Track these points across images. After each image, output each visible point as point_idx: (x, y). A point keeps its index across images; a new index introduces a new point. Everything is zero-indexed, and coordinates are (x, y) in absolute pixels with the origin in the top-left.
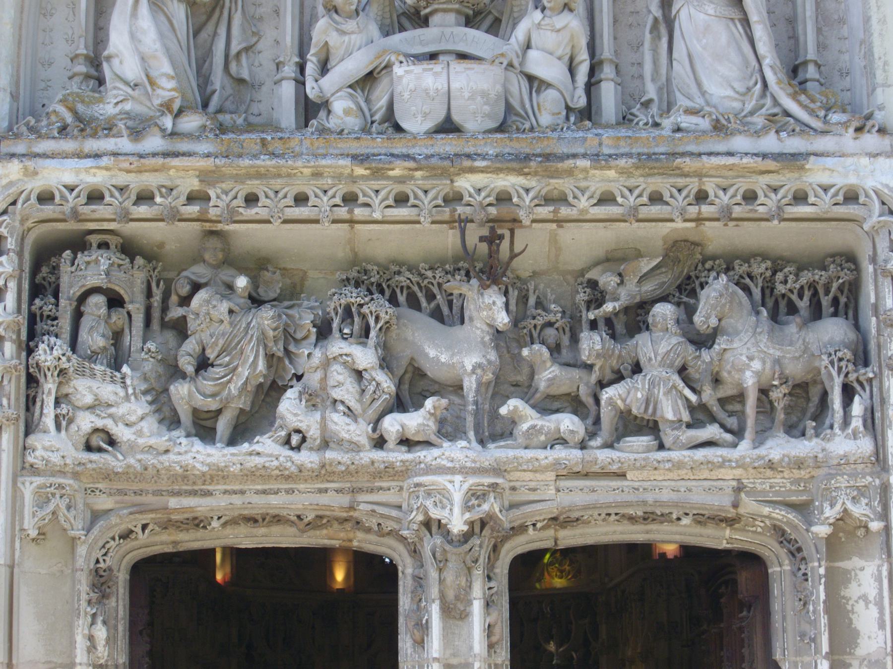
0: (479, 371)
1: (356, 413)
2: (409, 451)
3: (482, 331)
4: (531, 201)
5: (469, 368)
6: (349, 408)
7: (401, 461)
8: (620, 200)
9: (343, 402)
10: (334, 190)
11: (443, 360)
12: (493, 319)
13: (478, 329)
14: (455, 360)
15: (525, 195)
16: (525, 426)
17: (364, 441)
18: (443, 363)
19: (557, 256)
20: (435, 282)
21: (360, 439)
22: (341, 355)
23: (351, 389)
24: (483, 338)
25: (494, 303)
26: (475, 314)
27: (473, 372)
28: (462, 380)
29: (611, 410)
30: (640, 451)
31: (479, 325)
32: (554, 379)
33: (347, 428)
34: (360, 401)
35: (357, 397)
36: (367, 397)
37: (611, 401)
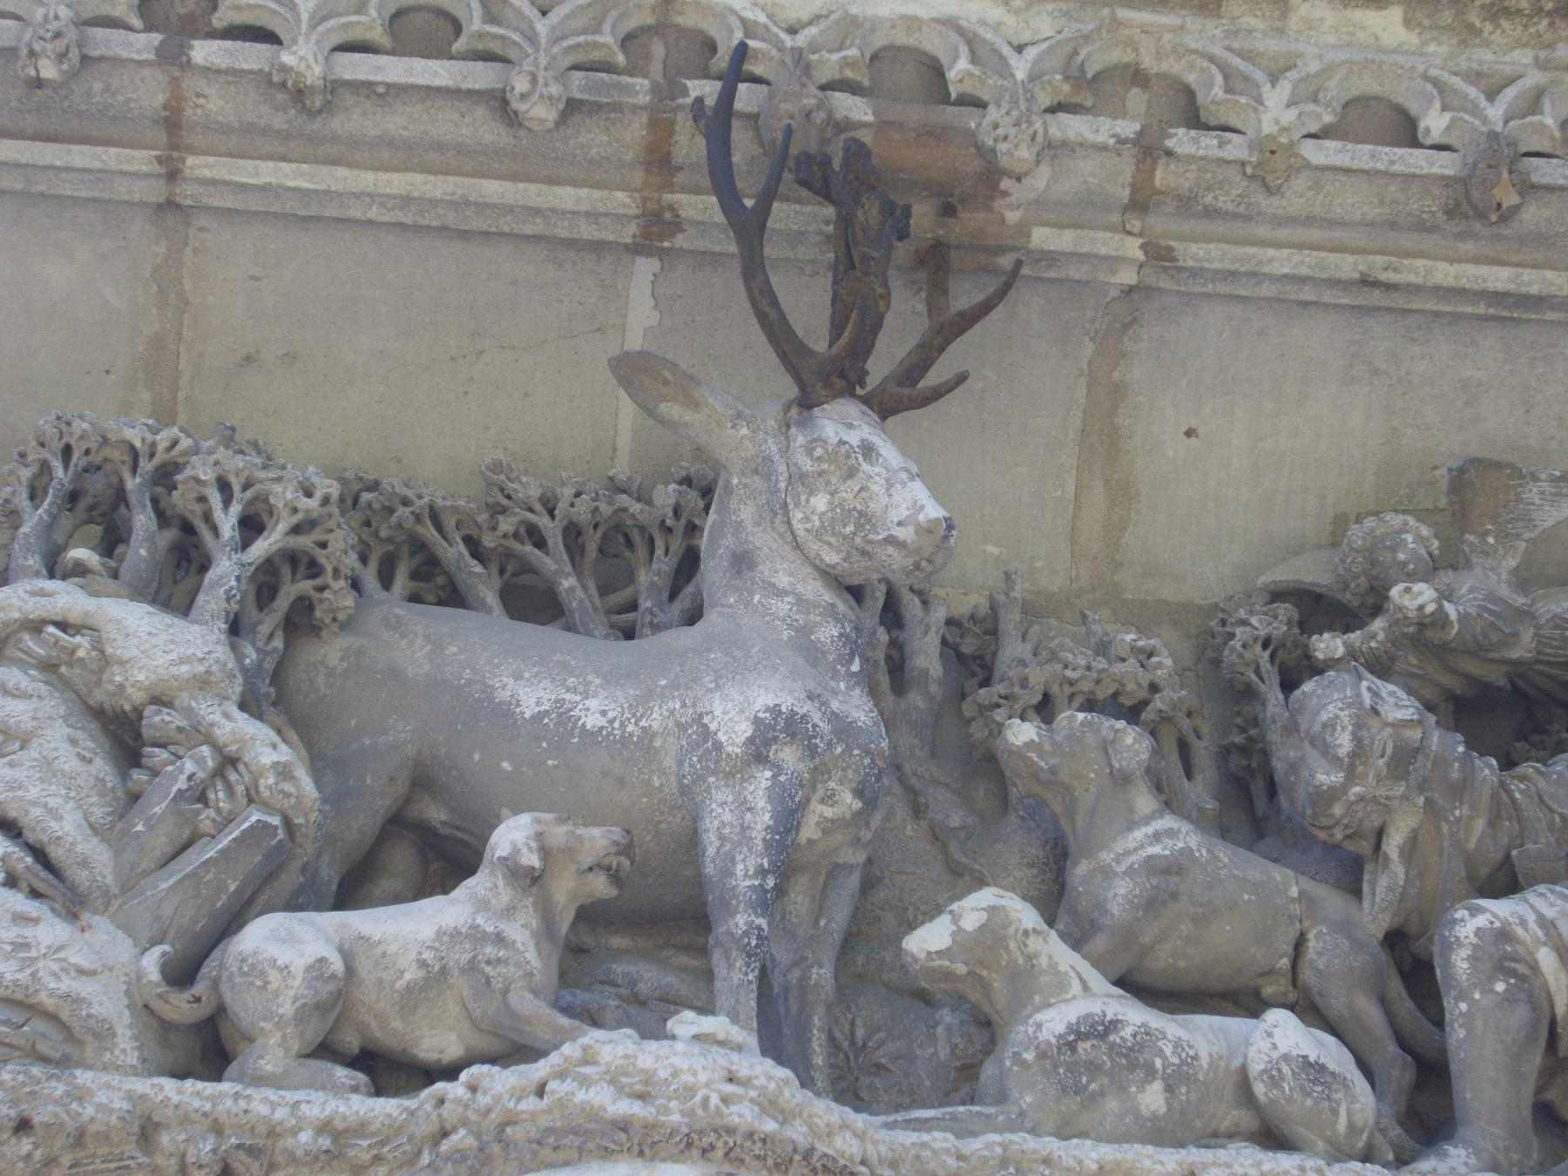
0: (789, 756)
1: (81, 877)
2: (379, 1091)
5: (734, 731)
6: (39, 854)
7: (324, 1127)
8: (1434, 123)
11: (592, 721)
12: (866, 519)
16: (1054, 1021)
17: (107, 1002)
18: (590, 736)
21: (84, 987)
22: (36, 627)
23: (68, 760)
24: (804, 631)
26: (763, 540)
27: (758, 752)
29: (1509, 999)
31: (783, 581)
34: (111, 831)
35: (99, 813)
36: (157, 816)
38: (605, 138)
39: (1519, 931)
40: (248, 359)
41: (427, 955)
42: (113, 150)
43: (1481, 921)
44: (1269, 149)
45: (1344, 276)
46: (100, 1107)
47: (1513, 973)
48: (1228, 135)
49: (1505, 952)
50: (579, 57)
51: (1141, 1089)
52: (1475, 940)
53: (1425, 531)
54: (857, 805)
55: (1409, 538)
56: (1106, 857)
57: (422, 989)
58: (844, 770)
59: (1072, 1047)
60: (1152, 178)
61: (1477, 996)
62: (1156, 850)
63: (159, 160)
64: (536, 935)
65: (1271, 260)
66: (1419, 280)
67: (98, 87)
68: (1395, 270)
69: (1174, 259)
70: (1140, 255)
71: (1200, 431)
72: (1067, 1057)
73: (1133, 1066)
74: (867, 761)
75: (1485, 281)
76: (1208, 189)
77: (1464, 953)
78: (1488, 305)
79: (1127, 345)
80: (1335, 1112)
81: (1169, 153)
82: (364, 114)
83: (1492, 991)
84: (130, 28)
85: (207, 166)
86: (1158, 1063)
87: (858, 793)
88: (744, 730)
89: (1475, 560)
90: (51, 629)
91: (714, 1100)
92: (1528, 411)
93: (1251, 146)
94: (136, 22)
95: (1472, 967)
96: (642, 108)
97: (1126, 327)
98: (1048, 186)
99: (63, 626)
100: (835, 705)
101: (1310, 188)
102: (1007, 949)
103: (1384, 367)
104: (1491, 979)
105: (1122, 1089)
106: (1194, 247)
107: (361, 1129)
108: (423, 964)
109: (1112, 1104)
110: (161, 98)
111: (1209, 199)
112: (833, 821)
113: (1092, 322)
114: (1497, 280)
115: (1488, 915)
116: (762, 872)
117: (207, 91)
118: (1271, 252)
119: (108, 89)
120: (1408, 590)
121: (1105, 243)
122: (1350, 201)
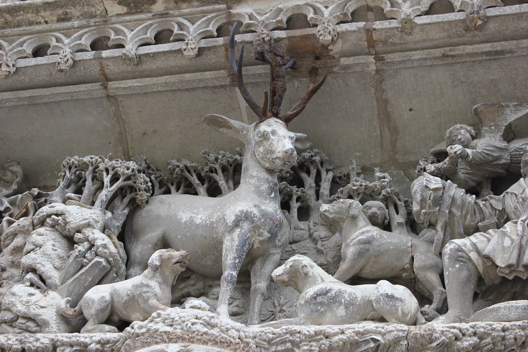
1: (48, 281)
3: (259, 179)
4: (331, 15)
5: (230, 219)
7: (99, 342)
9: (34, 271)
10: (80, 32)
11: (198, 221)
13: (253, 177)
14: (214, 219)
15: (323, 9)
16: (310, 291)
19: (393, 143)
20: (217, 166)
22: (49, 216)
24: (257, 187)
25: (274, 133)
27: (237, 224)
28: (221, 243)
29: (460, 269)
30: (512, 316)
31: (254, 173)
32: (368, 242)
33: (25, 298)
37: (460, 256)
38: (215, 56)
39: (464, 248)
40: (144, 134)
41: (129, 292)
42: (90, 84)
43: (452, 246)
44: (407, 21)
45: (437, 56)
46: (42, 343)
47: (462, 261)
48: (392, 20)
49: (459, 255)
50: (204, 36)
51: (337, 309)
52: (449, 252)
53: (469, 128)
54: (269, 235)
55: (462, 131)
56: (349, 241)
57: (128, 302)
58: (264, 226)
59: (315, 298)
60: (373, 37)
61: (451, 269)
62: (361, 237)
63: (102, 85)
64: (160, 284)
65: (414, 55)
66: (461, 53)
67: (82, 68)
68: (453, 51)
69: (384, 60)
70: (374, 61)
71: (414, 109)
72: (314, 301)
73: (335, 302)
74: (272, 222)
75: (482, 49)
76: (390, 37)
77: (447, 257)
78: (486, 56)
79: (384, 87)
80: (397, 310)
81: (374, 29)
82: (150, 62)
83: (455, 267)
84: (88, 51)
85: (113, 84)
86: (343, 300)
87: (269, 232)
88: (233, 218)
89: (486, 135)
90: (53, 216)
91: (190, 324)
92: (515, 86)
93: (399, 23)
94: (90, 49)
95: (450, 261)
96: (222, 46)
97: (381, 82)
98: (342, 46)
99: (57, 215)
100: (263, 207)
101: (420, 31)
102: (299, 272)
103: (464, 80)
104: (455, 264)
105: (332, 309)
106: (390, 55)
107: (108, 342)
108: (128, 295)
109: (329, 314)
110: (98, 68)
111: (391, 40)
112: (263, 241)
113: (371, 82)
114: (486, 48)
115: (454, 244)
116: (235, 258)
117: (109, 64)
118: (414, 52)
119: (84, 68)
120: (451, 148)
121: (362, 59)
122: (434, 33)
